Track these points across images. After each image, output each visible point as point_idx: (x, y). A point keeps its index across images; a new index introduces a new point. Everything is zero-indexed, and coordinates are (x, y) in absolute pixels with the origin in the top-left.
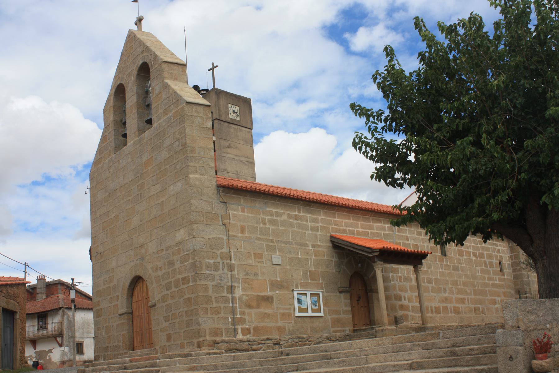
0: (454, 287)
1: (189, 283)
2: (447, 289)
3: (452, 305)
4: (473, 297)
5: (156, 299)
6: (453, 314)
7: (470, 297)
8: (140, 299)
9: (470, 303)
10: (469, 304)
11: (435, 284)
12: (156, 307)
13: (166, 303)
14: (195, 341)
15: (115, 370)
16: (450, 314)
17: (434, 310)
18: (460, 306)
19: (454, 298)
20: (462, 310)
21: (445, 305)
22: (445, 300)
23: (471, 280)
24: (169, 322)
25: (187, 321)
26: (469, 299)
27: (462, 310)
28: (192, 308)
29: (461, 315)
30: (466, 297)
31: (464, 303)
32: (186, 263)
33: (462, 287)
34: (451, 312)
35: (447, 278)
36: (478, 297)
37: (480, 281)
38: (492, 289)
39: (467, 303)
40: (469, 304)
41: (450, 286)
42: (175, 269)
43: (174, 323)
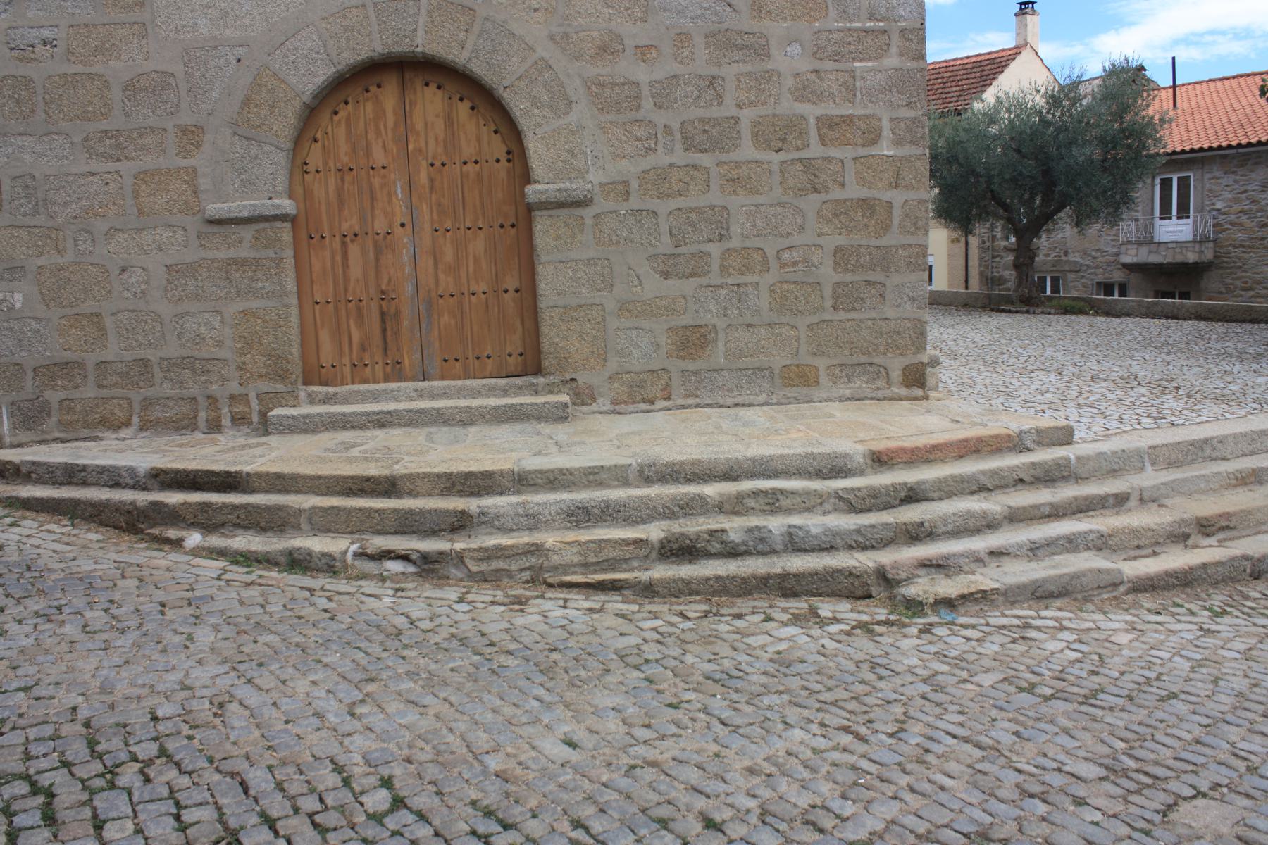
1: (874, 142)
5: (595, 177)
8: (379, 157)
12: (588, 213)
13: (673, 204)
14: (896, 365)
15: (827, 507)
24: (704, 281)
25: (837, 285)
28: (884, 241)
32: (857, 64)
42: (770, 76)
43: (738, 285)
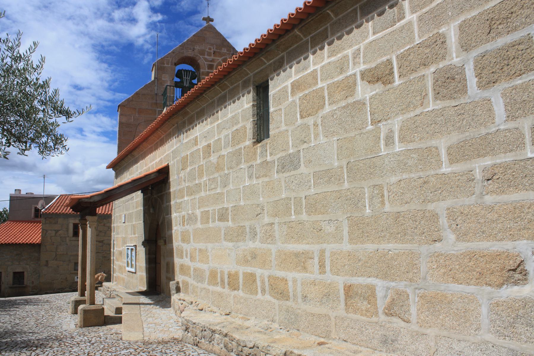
0: (277, 220)
2: (258, 230)
3: (266, 273)
4: (346, 246)
6: (268, 297)
7: (330, 247)
9: (328, 268)
10: (322, 271)
11: (233, 220)
16: (259, 296)
17: (226, 281)
18: (290, 275)
19: (274, 251)
20: (295, 290)
21: (249, 269)
22: (250, 259)
23: (346, 185)
26: (327, 254)
27: (295, 290)
29: (289, 303)
30: (315, 248)
31: (305, 269)
33: (304, 217)
34: (263, 291)
35: (261, 199)
36: (370, 247)
37: (394, 179)
38: (489, 199)
39: (317, 267)
40: (322, 271)
41: (267, 220)
